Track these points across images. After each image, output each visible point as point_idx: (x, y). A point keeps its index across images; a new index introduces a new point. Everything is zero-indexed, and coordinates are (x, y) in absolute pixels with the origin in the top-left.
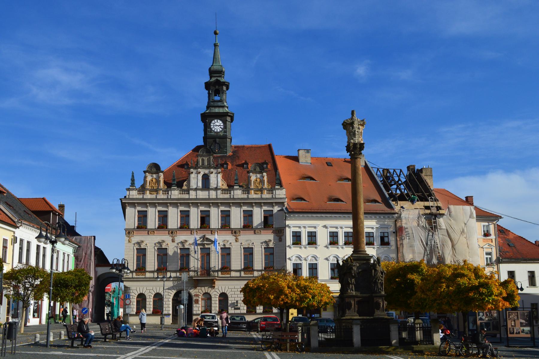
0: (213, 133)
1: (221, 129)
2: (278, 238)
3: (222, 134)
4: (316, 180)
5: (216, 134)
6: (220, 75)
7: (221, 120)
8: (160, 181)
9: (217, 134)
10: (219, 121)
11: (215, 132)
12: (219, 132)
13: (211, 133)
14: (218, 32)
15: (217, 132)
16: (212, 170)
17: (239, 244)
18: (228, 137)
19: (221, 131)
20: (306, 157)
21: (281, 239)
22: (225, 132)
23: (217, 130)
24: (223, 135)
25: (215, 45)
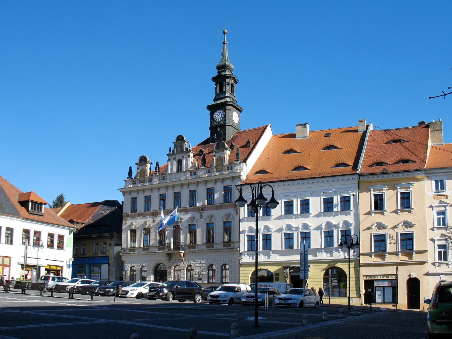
0: (215, 123)
1: (221, 118)
2: (235, 211)
3: (222, 123)
4: (298, 152)
5: (217, 124)
6: (224, 69)
7: (221, 109)
8: (146, 170)
9: (218, 124)
10: (220, 111)
11: (217, 122)
12: (220, 121)
13: (214, 123)
14: (226, 31)
15: (219, 122)
16: (183, 155)
17: (203, 220)
18: (227, 124)
19: (222, 120)
20: (303, 131)
21: (237, 212)
22: (225, 120)
23: (219, 120)
24: (223, 123)
25: (224, 43)
